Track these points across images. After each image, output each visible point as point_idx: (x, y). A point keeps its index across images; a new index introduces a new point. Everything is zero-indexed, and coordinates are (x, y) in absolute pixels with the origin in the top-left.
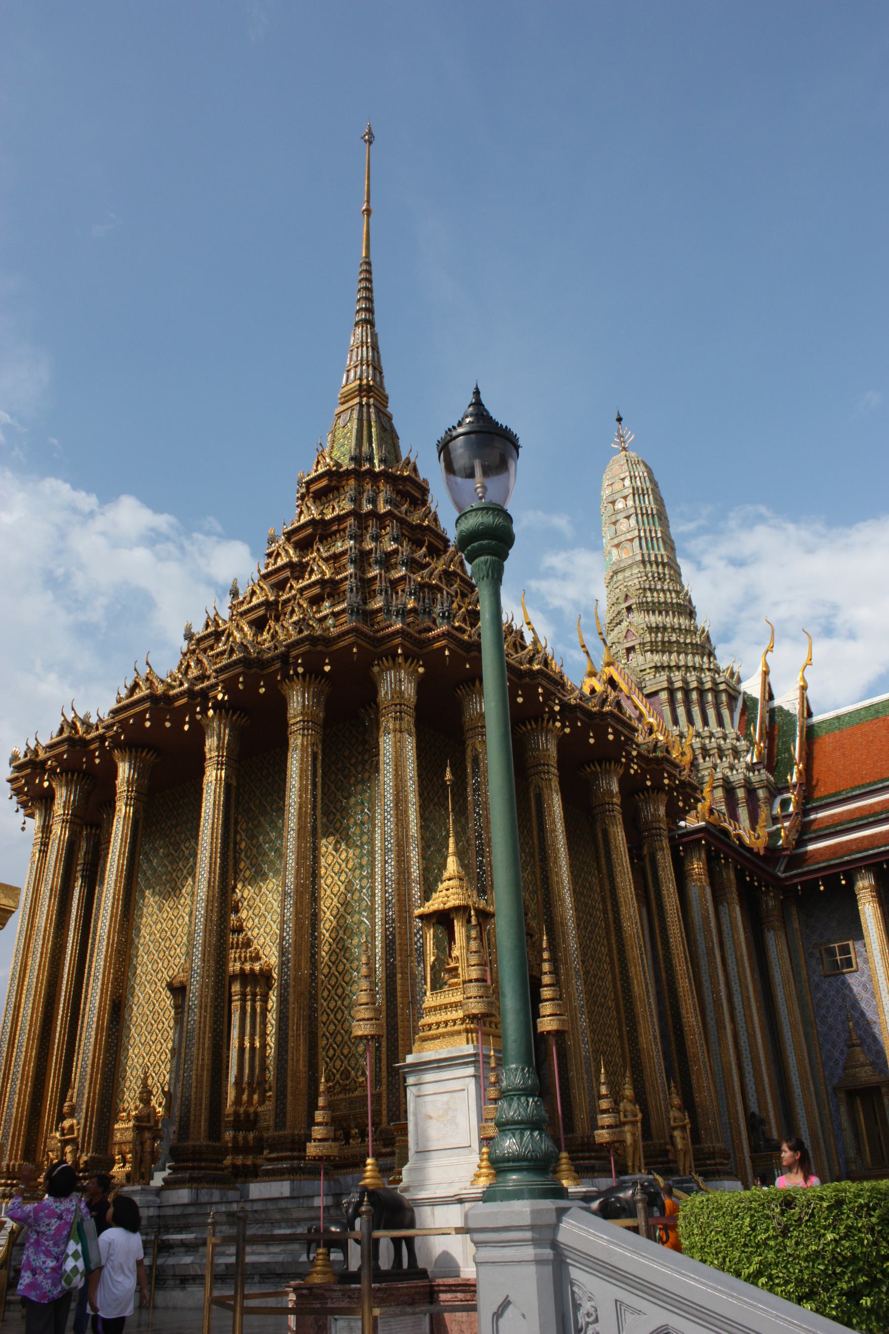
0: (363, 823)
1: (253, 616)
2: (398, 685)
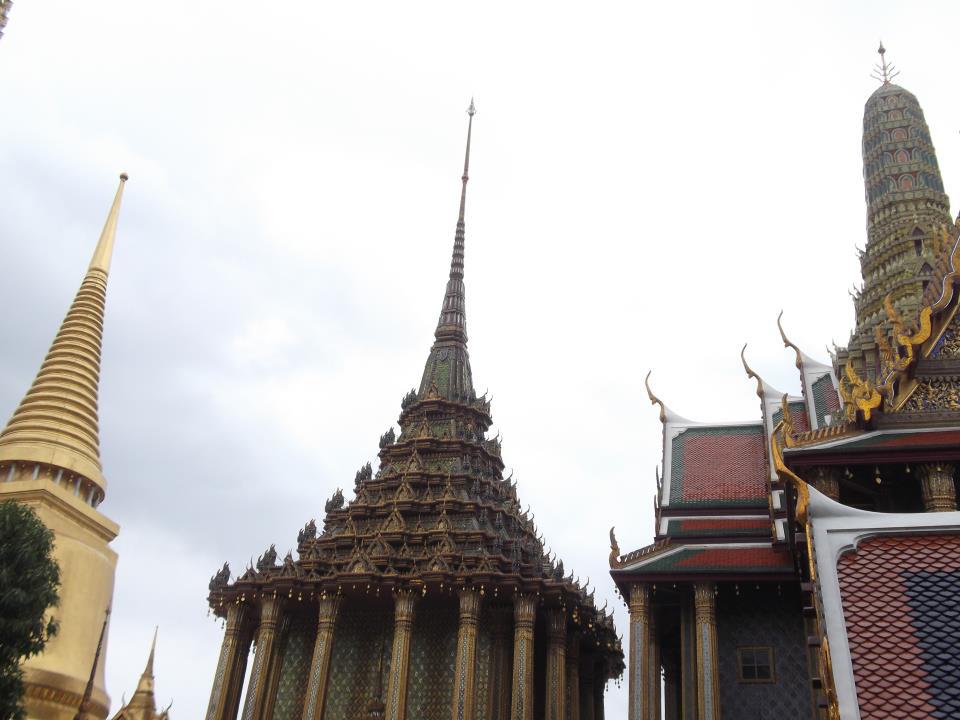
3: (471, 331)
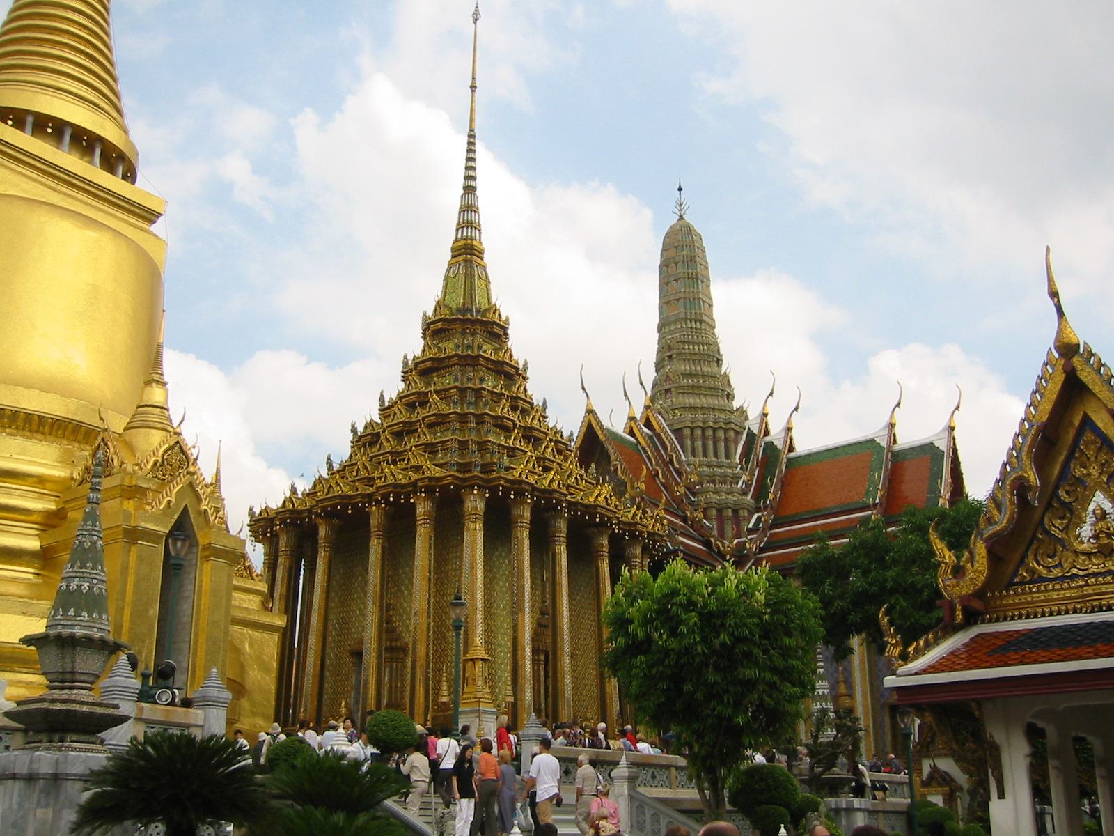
0: (456, 570)
1: (395, 429)
2: (475, 504)
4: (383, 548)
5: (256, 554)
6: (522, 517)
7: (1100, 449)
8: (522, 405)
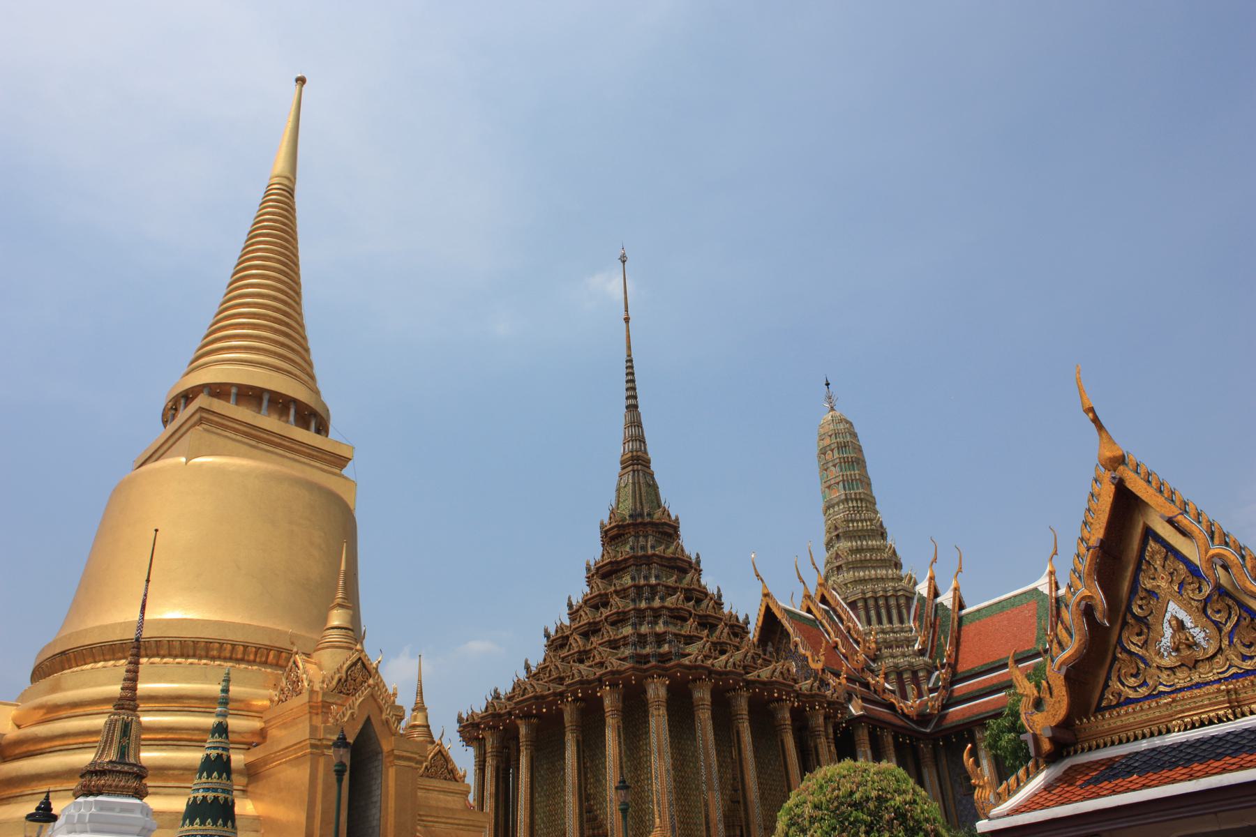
2: (657, 691)
3: (652, 453)
4: (578, 741)
5: (464, 759)
6: (703, 699)
7: (1166, 558)
8: (697, 595)
